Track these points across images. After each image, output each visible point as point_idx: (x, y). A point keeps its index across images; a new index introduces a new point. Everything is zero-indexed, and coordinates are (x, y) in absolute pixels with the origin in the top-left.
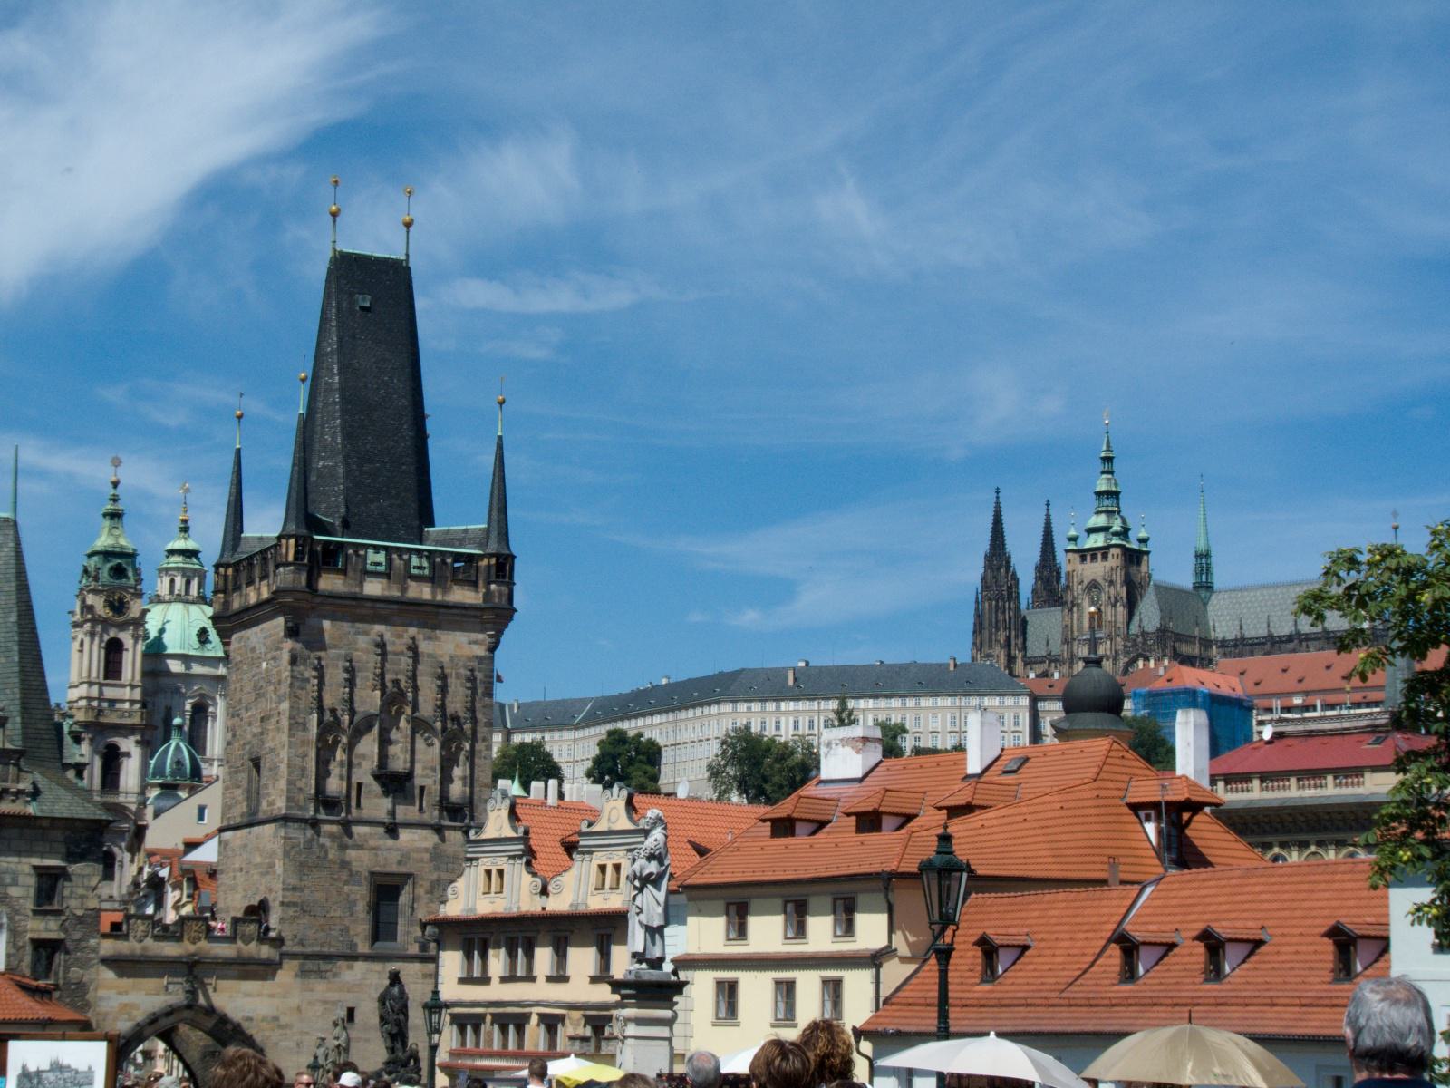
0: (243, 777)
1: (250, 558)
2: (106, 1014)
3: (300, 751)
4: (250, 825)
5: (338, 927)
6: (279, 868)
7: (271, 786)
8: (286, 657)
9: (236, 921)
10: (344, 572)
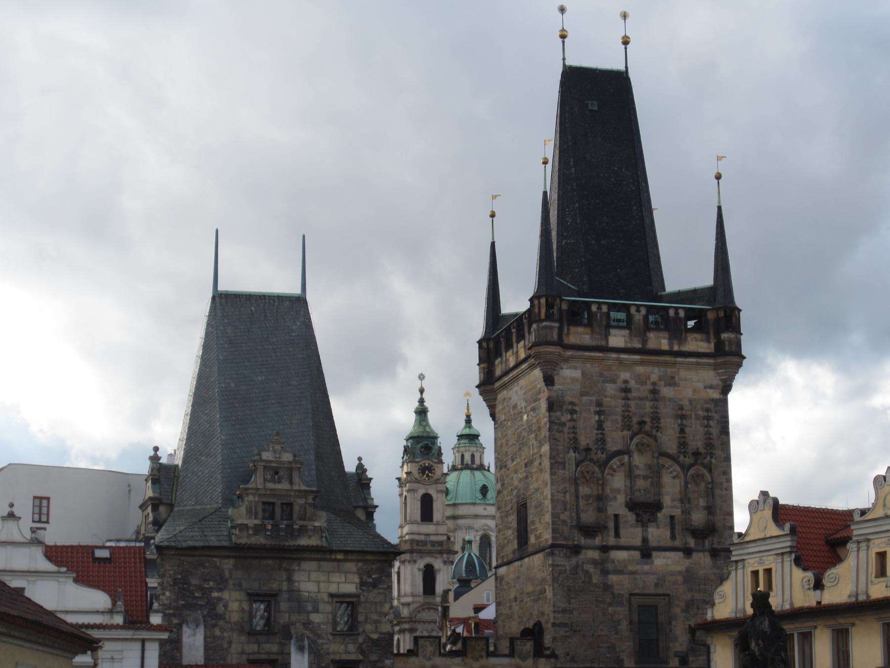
0: (513, 519)
1: (508, 330)
3: (562, 487)
4: (521, 558)
5: (605, 645)
6: (549, 594)
7: (537, 522)
8: (543, 405)
9: (512, 640)
10: (590, 325)
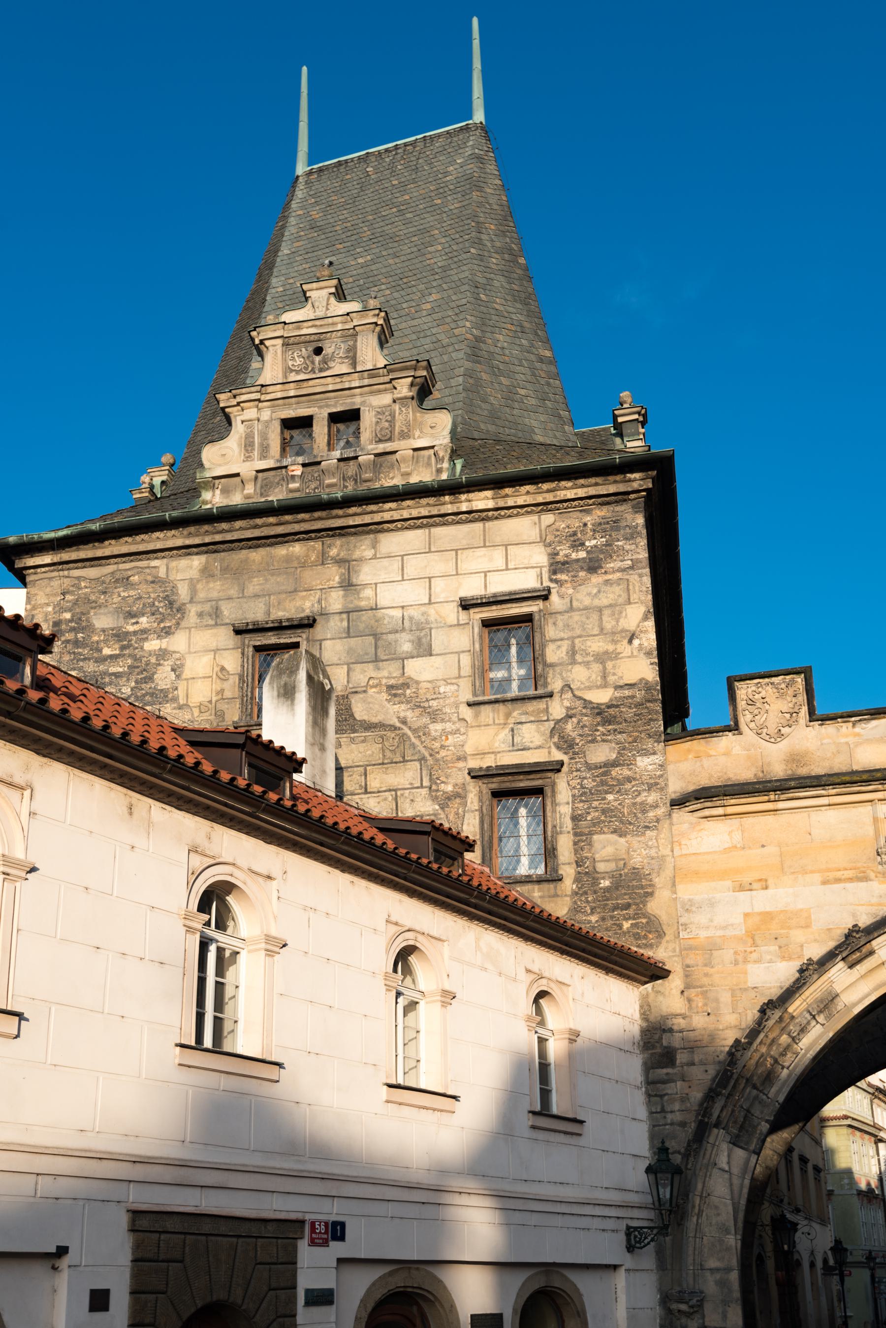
2: (711, 948)
